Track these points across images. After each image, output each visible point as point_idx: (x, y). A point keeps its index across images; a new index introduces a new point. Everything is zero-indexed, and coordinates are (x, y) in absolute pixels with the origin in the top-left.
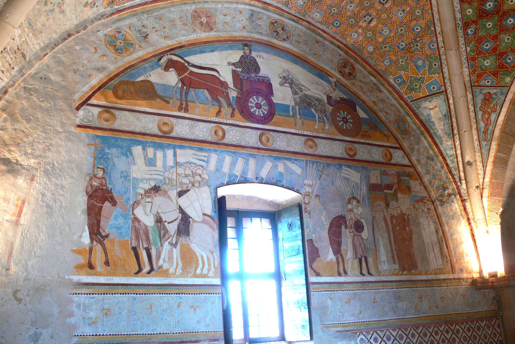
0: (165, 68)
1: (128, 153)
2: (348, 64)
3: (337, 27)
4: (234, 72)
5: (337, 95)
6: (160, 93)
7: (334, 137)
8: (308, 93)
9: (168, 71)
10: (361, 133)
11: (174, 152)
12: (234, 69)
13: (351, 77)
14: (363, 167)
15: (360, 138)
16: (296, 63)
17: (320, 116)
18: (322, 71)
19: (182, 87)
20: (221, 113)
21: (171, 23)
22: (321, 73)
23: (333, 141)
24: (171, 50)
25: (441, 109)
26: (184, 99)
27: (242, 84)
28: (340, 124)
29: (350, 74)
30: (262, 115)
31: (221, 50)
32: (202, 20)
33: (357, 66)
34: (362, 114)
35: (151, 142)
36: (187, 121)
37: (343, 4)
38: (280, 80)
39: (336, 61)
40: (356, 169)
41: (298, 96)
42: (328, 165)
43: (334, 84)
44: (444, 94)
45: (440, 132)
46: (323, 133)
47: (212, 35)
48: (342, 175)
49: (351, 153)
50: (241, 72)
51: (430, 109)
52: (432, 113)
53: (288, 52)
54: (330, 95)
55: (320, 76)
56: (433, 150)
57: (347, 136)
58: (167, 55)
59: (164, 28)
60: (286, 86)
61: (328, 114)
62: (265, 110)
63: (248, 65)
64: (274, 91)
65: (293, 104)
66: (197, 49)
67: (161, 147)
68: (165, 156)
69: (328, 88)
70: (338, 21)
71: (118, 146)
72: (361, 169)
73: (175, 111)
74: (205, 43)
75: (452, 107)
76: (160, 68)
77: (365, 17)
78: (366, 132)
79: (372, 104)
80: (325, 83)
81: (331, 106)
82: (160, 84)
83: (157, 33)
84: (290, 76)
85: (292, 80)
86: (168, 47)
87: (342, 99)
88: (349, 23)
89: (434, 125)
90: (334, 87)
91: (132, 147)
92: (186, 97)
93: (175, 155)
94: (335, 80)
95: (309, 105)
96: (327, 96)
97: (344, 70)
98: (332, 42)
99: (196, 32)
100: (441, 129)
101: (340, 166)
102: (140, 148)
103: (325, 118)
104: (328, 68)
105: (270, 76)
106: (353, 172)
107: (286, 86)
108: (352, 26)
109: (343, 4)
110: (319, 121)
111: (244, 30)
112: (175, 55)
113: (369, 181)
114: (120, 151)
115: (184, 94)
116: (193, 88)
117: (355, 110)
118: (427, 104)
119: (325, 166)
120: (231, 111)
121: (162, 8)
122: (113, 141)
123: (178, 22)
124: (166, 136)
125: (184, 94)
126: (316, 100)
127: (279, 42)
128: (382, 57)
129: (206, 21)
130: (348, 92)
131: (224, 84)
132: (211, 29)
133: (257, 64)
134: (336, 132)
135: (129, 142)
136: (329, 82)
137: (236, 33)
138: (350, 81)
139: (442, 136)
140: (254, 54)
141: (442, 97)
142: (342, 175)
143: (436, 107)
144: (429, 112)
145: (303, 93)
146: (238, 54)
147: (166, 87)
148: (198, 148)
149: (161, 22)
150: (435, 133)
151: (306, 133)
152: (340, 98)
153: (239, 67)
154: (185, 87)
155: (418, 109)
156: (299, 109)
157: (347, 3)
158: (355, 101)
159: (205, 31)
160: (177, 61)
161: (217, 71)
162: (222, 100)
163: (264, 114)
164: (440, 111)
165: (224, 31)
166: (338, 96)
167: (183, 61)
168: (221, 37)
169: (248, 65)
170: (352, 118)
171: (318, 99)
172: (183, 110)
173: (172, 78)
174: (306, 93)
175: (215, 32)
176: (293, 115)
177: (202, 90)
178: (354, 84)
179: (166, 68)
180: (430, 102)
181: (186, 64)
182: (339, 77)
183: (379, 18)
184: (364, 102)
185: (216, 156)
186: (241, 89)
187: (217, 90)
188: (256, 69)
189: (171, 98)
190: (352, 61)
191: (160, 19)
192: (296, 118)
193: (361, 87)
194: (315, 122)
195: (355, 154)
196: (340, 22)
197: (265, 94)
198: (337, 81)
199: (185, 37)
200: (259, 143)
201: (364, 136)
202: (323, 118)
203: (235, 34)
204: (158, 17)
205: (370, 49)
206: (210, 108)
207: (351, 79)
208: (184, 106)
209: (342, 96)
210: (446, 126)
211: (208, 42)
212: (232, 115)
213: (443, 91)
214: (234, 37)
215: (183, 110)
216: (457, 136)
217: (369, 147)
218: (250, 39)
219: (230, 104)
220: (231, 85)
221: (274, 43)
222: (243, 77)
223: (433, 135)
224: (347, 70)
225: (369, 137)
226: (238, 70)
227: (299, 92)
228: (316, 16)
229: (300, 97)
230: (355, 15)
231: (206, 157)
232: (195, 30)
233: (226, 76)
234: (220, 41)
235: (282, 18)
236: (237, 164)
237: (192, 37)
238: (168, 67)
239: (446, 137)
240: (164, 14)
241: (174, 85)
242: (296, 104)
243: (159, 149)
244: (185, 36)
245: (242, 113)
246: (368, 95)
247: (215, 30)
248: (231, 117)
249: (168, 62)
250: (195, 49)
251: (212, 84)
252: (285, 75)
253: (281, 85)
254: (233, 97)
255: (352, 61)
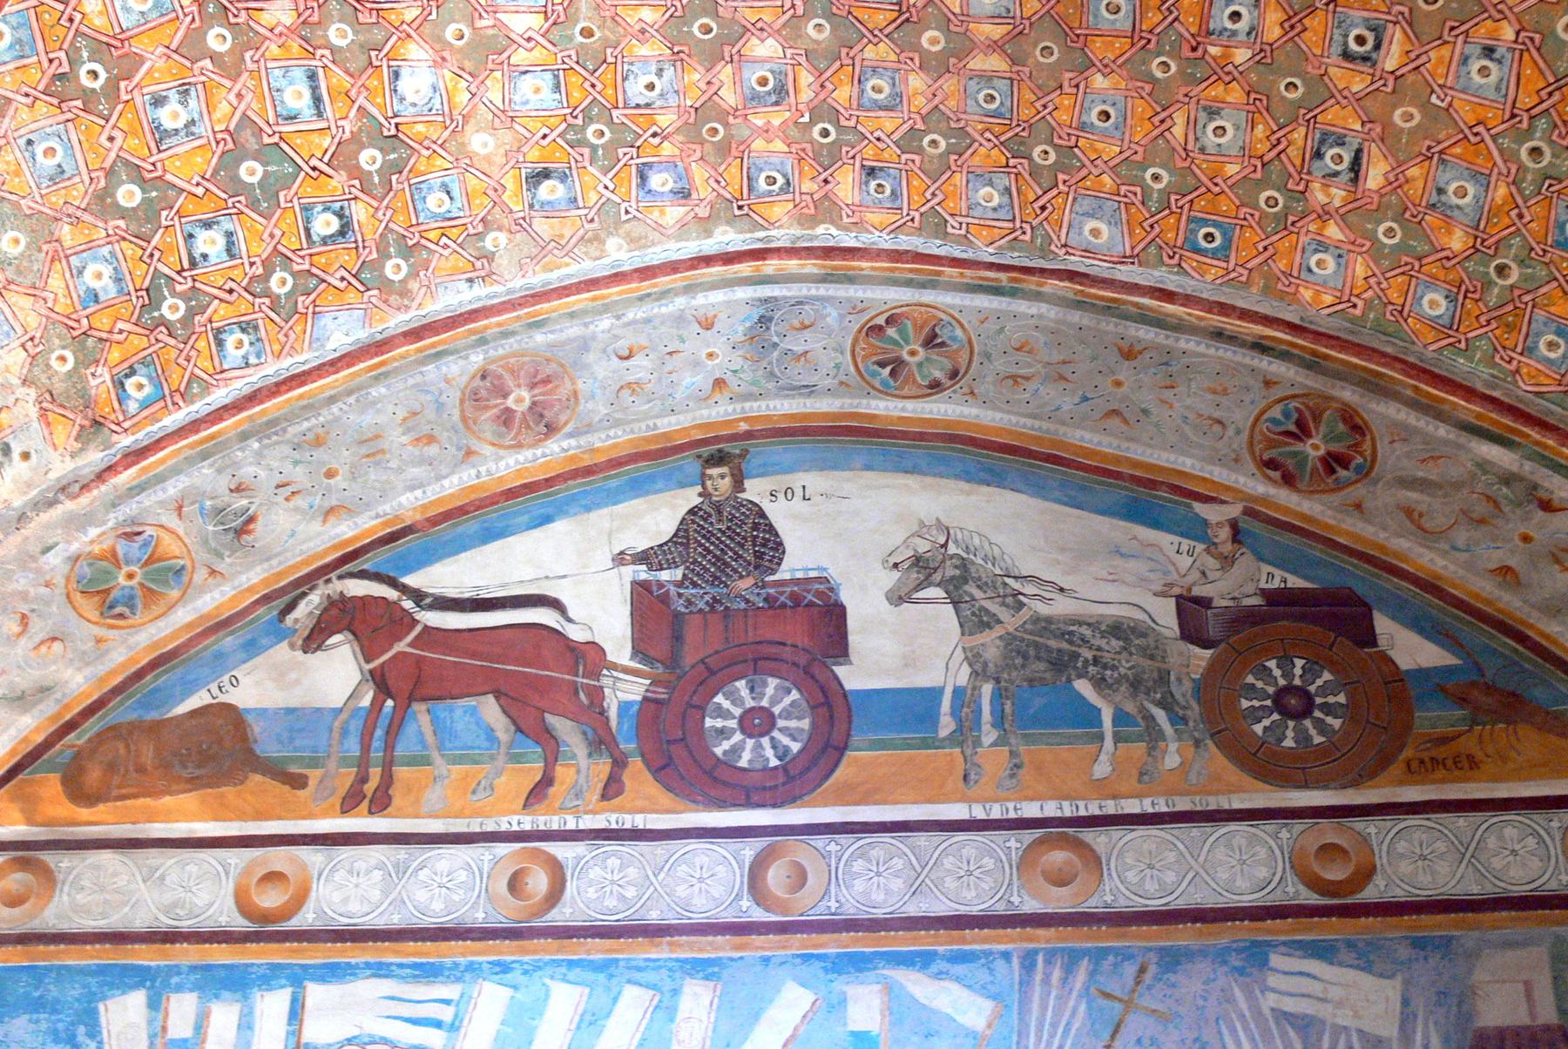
0: (308, 639)
1: (82, 1029)
2: (1317, 418)
3: (1223, 253)
4: (641, 590)
5: (1240, 582)
6: (268, 746)
7: (1213, 803)
8: (1061, 607)
9: (319, 648)
10: (1408, 753)
11: (294, 1000)
12: (643, 576)
13: (1342, 473)
14: (1418, 944)
15: (1401, 783)
16: (994, 478)
17: (1130, 707)
18: (1152, 484)
19: (377, 705)
20: (552, 791)
21: (364, 450)
22: (1147, 496)
23: (1207, 828)
24: (348, 560)
26: (377, 754)
27: (677, 638)
28: (1258, 729)
29: (1333, 462)
30: (774, 762)
31: (588, 509)
32: (510, 402)
33: (1381, 412)
34: (1409, 648)
35: (193, 969)
36: (377, 852)
37: (1178, 131)
38: (896, 575)
39: (1241, 417)
40: (1366, 959)
41: (998, 631)
42: (1172, 960)
43: (1225, 533)
46: (1140, 796)
47: (555, 451)
48: (1269, 1001)
49: (1335, 873)
50: (679, 584)
53: (952, 438)
54: (1197, 591)
55: (1136, 513)
57: (1305, 785)
58: (328, 581)
59: (330, 474)
60: (928, 601)
61: (1182, 691)
62: (793, 731)
63: (731, 539)
64: (853, 638)
65: (963, 676)
66: (470, 526)
67: (237, 983)
68: (246, 1025)
69: (1185, 562)
70: (1206, 222)
71: (37, 1005)
72: (1404, 952)
73: (325, 814)
74: (511, 494)
76: (285, 644)
77: (1318, 155)
78: (1444, 740)
79: (1484, 588)
80: (1166, 540)
81: (1206, 644)
82: (277, 711)
83: (298, 501)
84: (952, 549)
85: (964, 565)
86: (335, 547)
87: (1278, 599)
88: (1264, 215)
90: (1227, 548)
91: (104, 998)
92: (389, 746)
93: (296, 1013)
94: (1234, 511)
95: (1063, 664)
96: (1179, 597)
97: (1299, 447)
98: (1219, 335)
99: (473, 459)
101: (1257, 956)
102: (136, 1001)
103: (1160, 715)
104: (1187, 464)
105: (834, 573)
106: (1350, 975)
107: (928, 601)
108: (1285, 224)
109: (1178, 131)
110: (1118, 739)
111: (717, 397)
112: (363, 575)
113: (1466, 1016)
114: (44, 1026)
115: (379, 733)
116: (424, 699)
117: (1369, 638)
119: (1152, 970)
120: (607, 768)
121: (332, 400)
122: (22, 987)
123: (397, 439)
124: (265, 930)
125: (379, 733)
126: (1103, 635)
127: (900, 404)
128: (1510, 327)
129: (527, 403)
130: (1317, 552)
131: (588, 657)
132: (551, 429)
133: (771, 529)
134: (1232, 773)
135: (93, 981)
136: (1197, 530)
137: (673, 419)
138: (1335, 498)
140: (755, 490)
142: (1269, 1001)
145: (1025, 614)
146: (673, 507)
147: (298, 718)
148: (415, 966)
149: (319, 454)
151: (1031, 810)
152: (1264, 593)
153: (672, 565)
154: (390, 703)
156: (999, 696)
157: (1192, 123)
158: (1360, 589)
159: (519, 446)
160: (366, 601)
161: (555, 604)
162: (561, 726)
163: (782, 753)
165: (617, 423)
166: (1250, 588)
167: (392, 594)
168: (593, 451)
169: (731, 539)
170: (1343, 685)
171: (1117, 629)
172: (365, 803)
173: (336, 675)
174: (1043, 609)
175: (570, 435)
176: (960, 728)
177: (471, 702)
178: (1358, 506)
179: (314, 640)
181: (408, 604)
182: (1260, 488)
183: (1388, 136)
184: (1431, 586)
185: (507, 992)
186: (672, 662)
187: (544, 687)
188: (759, 556)
189: (315, 763)
190: (1348, 394)
191: (318, 442)
192: (977, 742)
193: (1409, 512)
194: (1094, 747)
195: (1366, 874)
196: (1216, 225)
197: (802, 660)
198: (1249, 512)
199: (418, 493)
200: (746, 903)
201: (1418, 770)
202: (1149, 719)
203: (667, 424)
204: (310, 436)
205: (1433, 304)
206: (499, 774)
207: (1340, 487)
208: (370, 787)
209: (1276, 584)
211: (529, 488)
212: (612, 789)
214: (666, 436)
215: (365, 803)
217: (1462, 822)
218: (744, 427)
219: (601, 741)
220: (619, 650)
221: (873, 417)
222: (689, 603)
224: (1314, 449)
225: (1468, 765)
226: (665, 576)
227: (1003, 614)
228: (1095, 233)
229: (1009, 640)
230: (1264, 166)
231: (447, 1002)
232: (469, 453)
233: (602, 615)
234: (589, 471)
235: (928, 296)
236: (611, 1023)
237: (454, 484)
238: (322, 631)
240: (337, 419)
241: (340, 705)
242: (980, 672)
243: (226, 994)
244: (421, 486)
245: (662, 769)
246: (1460, 543)
247: (568, 429)
248: (605, 796)
249: (326, 610)
250: (460, 529)
251: (528, 668)
252: (923, 547)
253: (898, 598)
254: (624, 707)
255: (1348, 394)
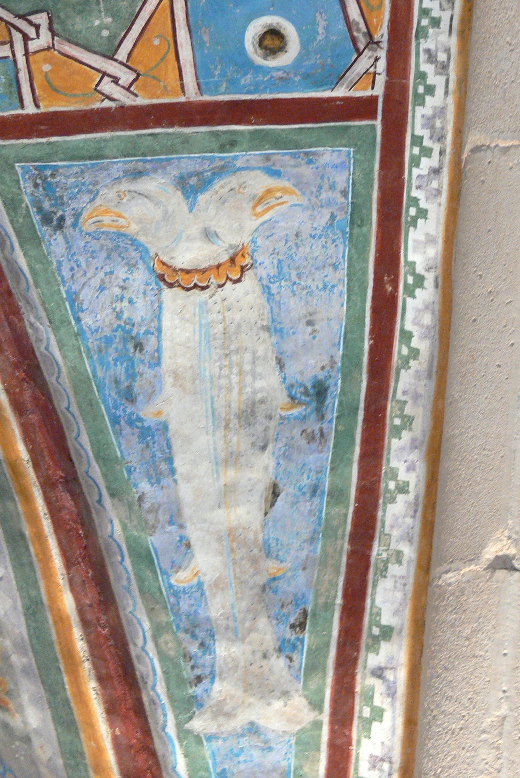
25: (295, 307)
44: (362, 144)
45: (207, 562)
51: (169, 277)
52: (180, 321)
56: (66, 718)
75: (416, 312)
89: (162, 466)
100: (232, 537)
118: (151, 208)
139: (216, 608)
141: (338, 163)
143: (237, 265)
144: (140, 311)
150: (144, 557)
155: (30, 239)
164: (275, 328)
180: (191, 187)
210: (298, 518)
213: (363, 108)
216: (386, 661)
223: (123, 571)
239: (266, 633)
